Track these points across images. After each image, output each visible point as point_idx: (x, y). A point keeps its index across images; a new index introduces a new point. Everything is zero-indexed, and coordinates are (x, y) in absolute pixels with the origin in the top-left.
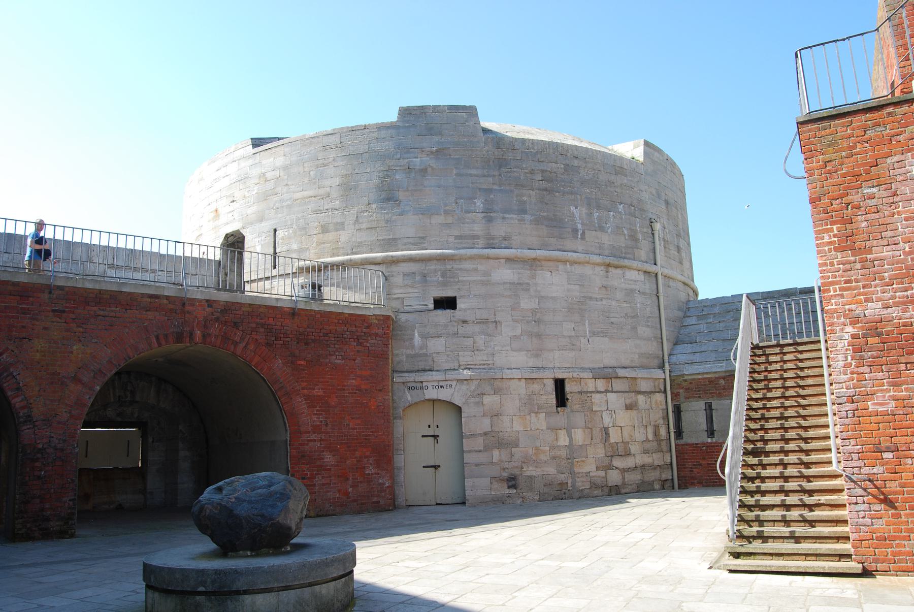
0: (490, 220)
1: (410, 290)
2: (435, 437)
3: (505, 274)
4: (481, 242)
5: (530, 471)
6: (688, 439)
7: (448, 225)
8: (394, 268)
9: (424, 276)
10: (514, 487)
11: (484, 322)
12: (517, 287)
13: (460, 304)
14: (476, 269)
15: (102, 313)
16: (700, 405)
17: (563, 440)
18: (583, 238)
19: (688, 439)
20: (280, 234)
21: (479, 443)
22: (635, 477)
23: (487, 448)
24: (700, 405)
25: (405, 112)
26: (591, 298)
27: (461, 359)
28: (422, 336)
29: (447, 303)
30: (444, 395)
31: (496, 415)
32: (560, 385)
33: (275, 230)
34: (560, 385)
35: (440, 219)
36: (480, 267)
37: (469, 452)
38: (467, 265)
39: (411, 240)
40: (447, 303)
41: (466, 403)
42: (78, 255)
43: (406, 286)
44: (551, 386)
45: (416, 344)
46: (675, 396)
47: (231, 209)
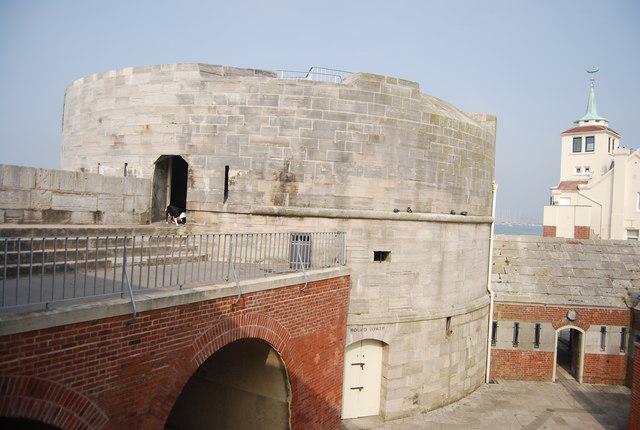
0: (419, 186)
1: (358, 244)
2: (362, 365)
3: (425, 233)
5: (428, 389)
6: (500, 345)
8: (346, 223)
9: (369, 234)
13: (394, 258)
14: (406, 230)
17: (447, 364)
19: (500, 345)
20: (232, 173)
21: (399, 372)
23: (405, 375)
24: (511, 323)
29: (380, 256)
30: (377, 336)
31: (410, 348)
33: (227, 168)
36: (410, 228)
38: (401, 225)
39: (361, 200)
40: (380, 256)
41: (393, 342)
42: (27, 182)
46: (495, 315)
47: (169, 130)
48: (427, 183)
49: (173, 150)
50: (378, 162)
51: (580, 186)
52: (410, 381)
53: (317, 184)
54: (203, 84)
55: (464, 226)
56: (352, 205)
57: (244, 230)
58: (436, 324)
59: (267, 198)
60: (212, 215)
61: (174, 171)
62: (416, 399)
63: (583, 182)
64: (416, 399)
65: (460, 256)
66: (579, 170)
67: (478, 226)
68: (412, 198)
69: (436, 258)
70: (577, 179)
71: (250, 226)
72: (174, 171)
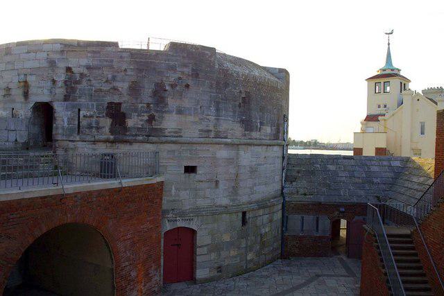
3: (223, 153)
4: (212, 134)
7: (194, 123)
10: (220, 271)
11: (210, 181)
12: (230, 161)
13: (200, 171)
15: (11, 217)
16: (299, 217)
18: (260, 131)
22: (270, 256)
25: (174, 46)
26: (260, 165)
27: (198, 203)
28: (176, 189)
29: (190, 170)
32: (244, 213)
34: (244, 213)
35: (191, 118)
37: (199, 255)
39: (173, 130)
43: (169, 158)
44: (240, 215)
45: (173, 194)
47: (40, 85)
48: (223, 118)
49: (45, 99)
50: (187, 103)
51: (380, 118)
52: (213, 256)
53: (142, 120)
54: (62, 52)
55: (256, 147)
56: (167, 134)
57: (90, 152)
58: (234, 216)
59: (107, 130)
60: (70, 143)
61: (45, 112)
62: (219, 269)
63: (382, 115)
64: (219, 269)
65: (253, 171)
66: (379, 106)
67: (269, 147)
68: (211, 128)
69: (232, 171)
70: (377, 113)
71: (95, 150)
72: (45, 112)
